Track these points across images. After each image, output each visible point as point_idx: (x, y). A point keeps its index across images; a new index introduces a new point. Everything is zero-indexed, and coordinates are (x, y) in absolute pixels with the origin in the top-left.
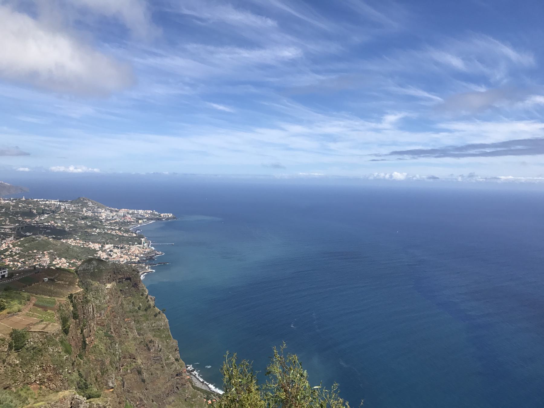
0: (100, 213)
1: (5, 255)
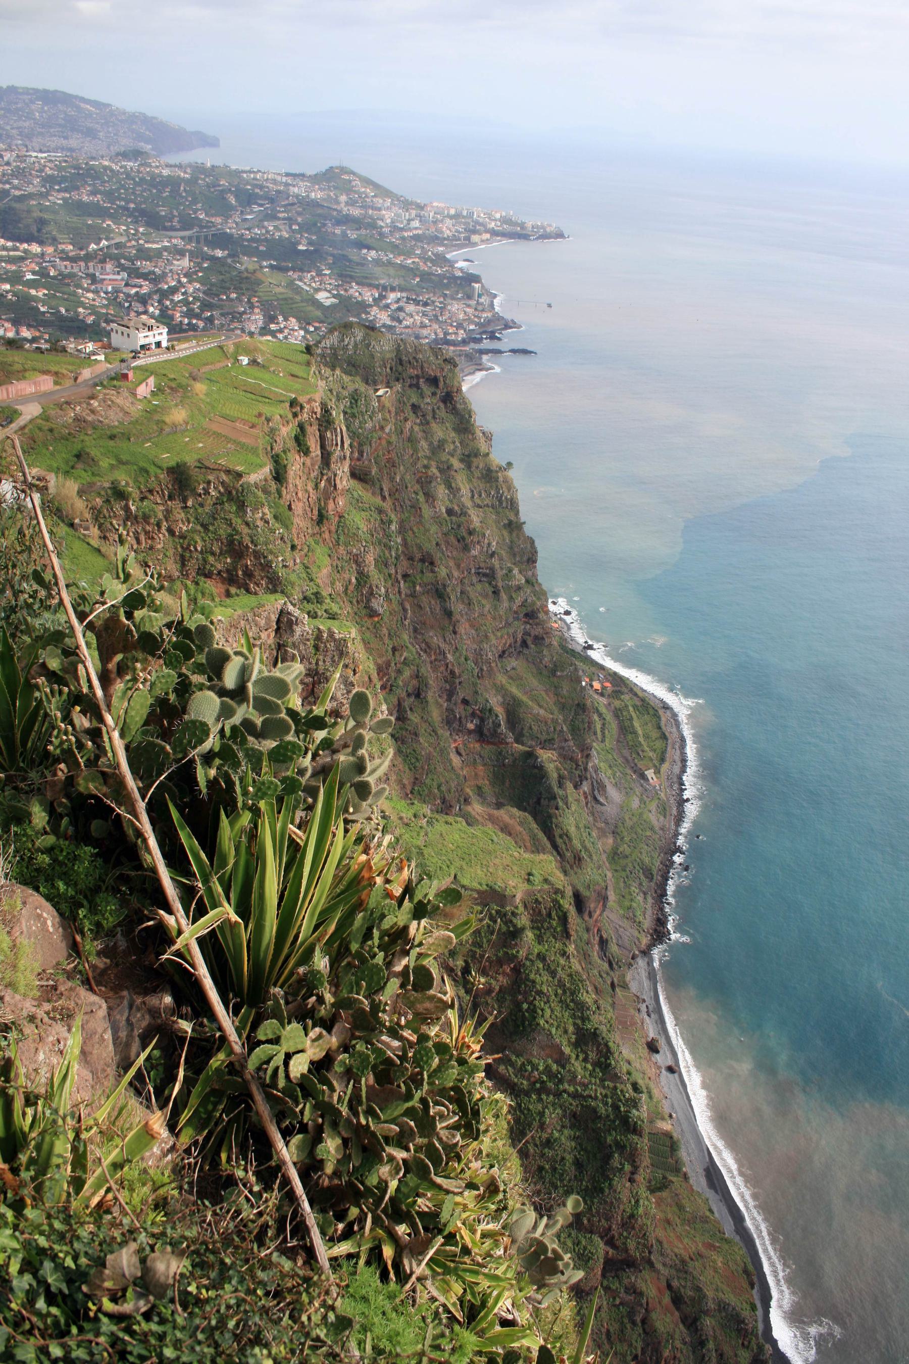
0: (380, 209)
1: (172, 301)
